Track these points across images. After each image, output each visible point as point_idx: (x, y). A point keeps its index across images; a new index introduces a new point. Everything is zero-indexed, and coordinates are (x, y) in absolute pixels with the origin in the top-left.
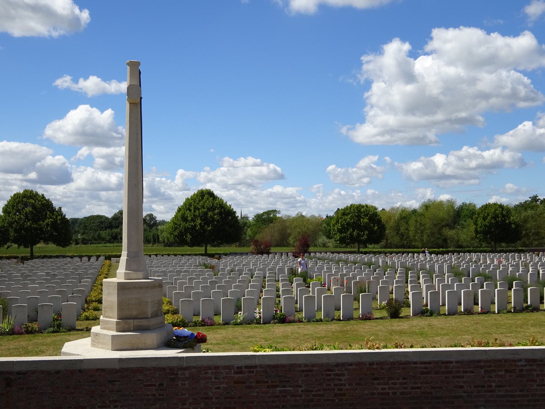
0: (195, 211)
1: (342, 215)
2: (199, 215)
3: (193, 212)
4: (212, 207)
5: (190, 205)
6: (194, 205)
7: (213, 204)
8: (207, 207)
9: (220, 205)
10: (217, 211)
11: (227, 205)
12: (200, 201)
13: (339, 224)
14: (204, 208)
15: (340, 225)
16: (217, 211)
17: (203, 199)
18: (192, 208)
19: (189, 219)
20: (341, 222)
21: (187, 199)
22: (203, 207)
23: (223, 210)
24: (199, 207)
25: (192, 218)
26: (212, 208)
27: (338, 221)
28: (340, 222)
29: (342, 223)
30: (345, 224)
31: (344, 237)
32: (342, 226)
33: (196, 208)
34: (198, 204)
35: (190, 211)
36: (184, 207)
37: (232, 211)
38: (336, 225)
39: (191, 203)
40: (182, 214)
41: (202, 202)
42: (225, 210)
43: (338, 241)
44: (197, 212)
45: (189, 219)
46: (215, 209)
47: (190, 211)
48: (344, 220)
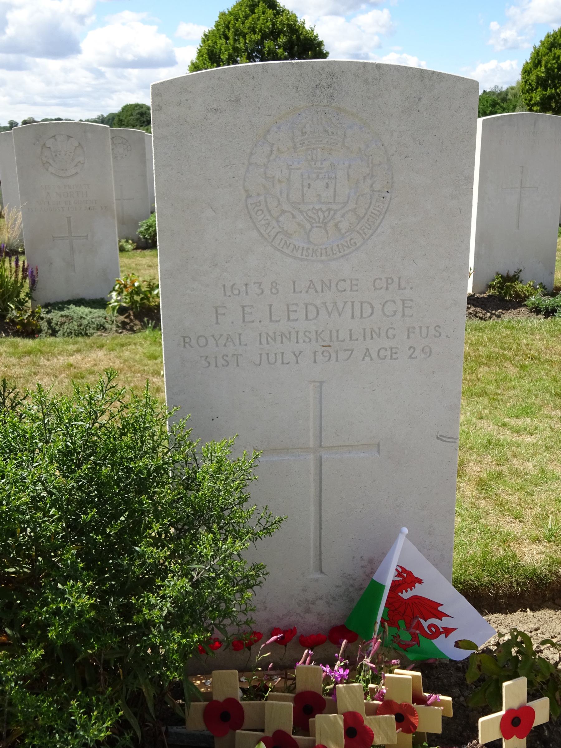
0: (235, 40)
1: (550, 49)
2: (246, 49)
3: (231, 41)
4: (273, 30)
5: (228, 27)
6: (234, 25)
7: (274, 25)
8: (260, 30)
9: (288, 25)
10: (282, 40)
11: (304, 27)
12: (246, 17)
13: (541, 67)
14: (255, 33)
15: (543, 69)
16: (282, 40)
17: (253, 12)
18: (230, 34)
19: (224, 57)
20: (547, 63)
21: (222, 15)
22: (253, 30)
23: (295, 37)
24: (246, 31)
25: (230, 55)
26: (272, 33)
27: (540, 62)
28: (543, 63)
29: (549, 65)
30: (556, 66)
31: (551, 97)
32: (548, 70)
33: (239, 33)
34: (243, 23)
35: (227, 38)
36: (216, 32)
37: (315, 40)
38: (536, 71)
39: (229, 22)
40: (209, 46)
41: (250, 19)
42: (298, 38)
43: (535, 104)
44: (241, 40)
45: (224, 57)
46: (278, 36)
47: (227, 38)
48: (553, 59)
